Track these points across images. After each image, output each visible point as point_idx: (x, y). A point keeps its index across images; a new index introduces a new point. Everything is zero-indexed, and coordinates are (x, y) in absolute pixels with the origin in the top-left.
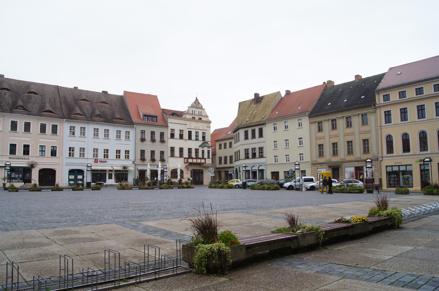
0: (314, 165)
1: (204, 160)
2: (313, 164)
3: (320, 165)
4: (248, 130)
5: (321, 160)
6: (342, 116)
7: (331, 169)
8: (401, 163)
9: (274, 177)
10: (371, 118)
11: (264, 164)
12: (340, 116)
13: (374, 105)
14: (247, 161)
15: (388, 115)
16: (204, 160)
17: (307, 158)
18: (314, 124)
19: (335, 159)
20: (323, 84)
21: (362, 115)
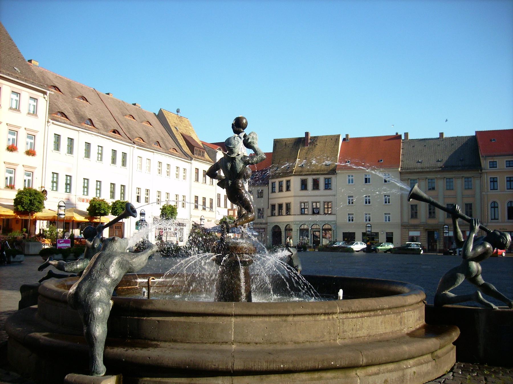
0: (404, 227)
1: (232, 211)
2: (403, 226)
3: (413, 227)
4: (319, 178)
5: (414, 222)
6: (443, 176)
7: (427, 232)
8: (506, 229)
9: (346, 239)
10: (476, 182)
11: (332, 222)
12: (439, 176)
13: (481, 170)
14: (303, 218)
15: (494, 181)
16: (232, 211)
17: (396, 218)
18: (407, 181)
19: (432, 222)
20: (395, 134)
21: (465, 178)
